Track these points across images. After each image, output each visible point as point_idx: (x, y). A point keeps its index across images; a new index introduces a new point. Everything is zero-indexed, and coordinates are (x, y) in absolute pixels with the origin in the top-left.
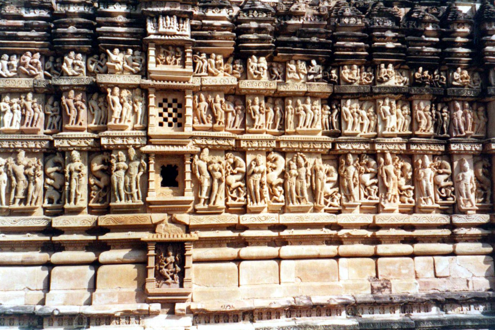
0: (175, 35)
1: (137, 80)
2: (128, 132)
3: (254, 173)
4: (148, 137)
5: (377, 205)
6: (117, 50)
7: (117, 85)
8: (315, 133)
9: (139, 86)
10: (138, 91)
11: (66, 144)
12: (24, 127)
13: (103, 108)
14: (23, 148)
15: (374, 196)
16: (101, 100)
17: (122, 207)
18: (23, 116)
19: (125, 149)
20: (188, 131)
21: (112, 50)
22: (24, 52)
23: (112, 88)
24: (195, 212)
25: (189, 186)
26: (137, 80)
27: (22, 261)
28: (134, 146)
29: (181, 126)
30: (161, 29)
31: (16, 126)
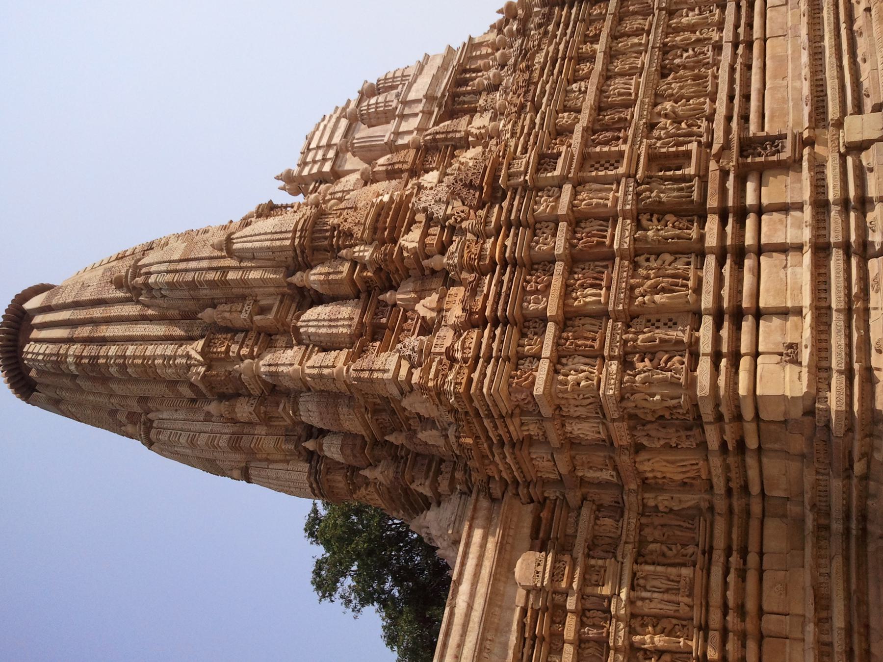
0: (528, 163)
1: (567, 188)
2: (620, 194)
3: (674, 112)
4: (628, 176)
5: (714, 48)
6: (535, 207)
7: (571, 202)
8: (638, 84)
9: (574, 187)
10: (579, 188)
11: (627, 240)
12: (604, 283)
13: (592, 224)
14: (627, 282)
15: (706, 49)
16: (583, 225)
17: (700, 194)
18: (592, 286)
19: (638, 194)
20: (625, 148)
21: (534, 211)
22: (524, 288)
23: (573, 206)
24: (710, 145)
25: (683, 148)
26: (567, 188)
27: (753, 274)
28: (635, 188)
29: (621, 154)
30: (522, 169)
31: (603, 292)
